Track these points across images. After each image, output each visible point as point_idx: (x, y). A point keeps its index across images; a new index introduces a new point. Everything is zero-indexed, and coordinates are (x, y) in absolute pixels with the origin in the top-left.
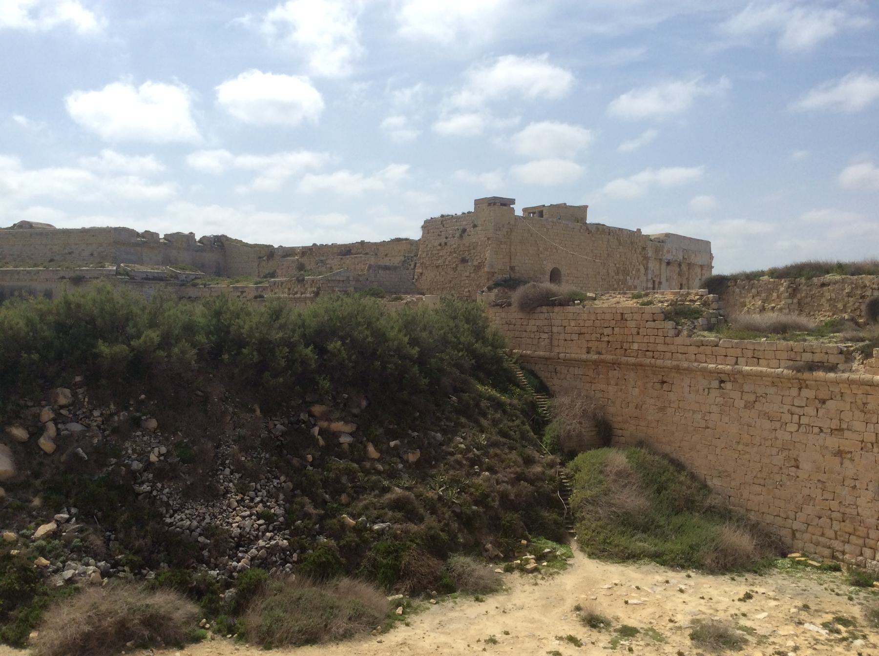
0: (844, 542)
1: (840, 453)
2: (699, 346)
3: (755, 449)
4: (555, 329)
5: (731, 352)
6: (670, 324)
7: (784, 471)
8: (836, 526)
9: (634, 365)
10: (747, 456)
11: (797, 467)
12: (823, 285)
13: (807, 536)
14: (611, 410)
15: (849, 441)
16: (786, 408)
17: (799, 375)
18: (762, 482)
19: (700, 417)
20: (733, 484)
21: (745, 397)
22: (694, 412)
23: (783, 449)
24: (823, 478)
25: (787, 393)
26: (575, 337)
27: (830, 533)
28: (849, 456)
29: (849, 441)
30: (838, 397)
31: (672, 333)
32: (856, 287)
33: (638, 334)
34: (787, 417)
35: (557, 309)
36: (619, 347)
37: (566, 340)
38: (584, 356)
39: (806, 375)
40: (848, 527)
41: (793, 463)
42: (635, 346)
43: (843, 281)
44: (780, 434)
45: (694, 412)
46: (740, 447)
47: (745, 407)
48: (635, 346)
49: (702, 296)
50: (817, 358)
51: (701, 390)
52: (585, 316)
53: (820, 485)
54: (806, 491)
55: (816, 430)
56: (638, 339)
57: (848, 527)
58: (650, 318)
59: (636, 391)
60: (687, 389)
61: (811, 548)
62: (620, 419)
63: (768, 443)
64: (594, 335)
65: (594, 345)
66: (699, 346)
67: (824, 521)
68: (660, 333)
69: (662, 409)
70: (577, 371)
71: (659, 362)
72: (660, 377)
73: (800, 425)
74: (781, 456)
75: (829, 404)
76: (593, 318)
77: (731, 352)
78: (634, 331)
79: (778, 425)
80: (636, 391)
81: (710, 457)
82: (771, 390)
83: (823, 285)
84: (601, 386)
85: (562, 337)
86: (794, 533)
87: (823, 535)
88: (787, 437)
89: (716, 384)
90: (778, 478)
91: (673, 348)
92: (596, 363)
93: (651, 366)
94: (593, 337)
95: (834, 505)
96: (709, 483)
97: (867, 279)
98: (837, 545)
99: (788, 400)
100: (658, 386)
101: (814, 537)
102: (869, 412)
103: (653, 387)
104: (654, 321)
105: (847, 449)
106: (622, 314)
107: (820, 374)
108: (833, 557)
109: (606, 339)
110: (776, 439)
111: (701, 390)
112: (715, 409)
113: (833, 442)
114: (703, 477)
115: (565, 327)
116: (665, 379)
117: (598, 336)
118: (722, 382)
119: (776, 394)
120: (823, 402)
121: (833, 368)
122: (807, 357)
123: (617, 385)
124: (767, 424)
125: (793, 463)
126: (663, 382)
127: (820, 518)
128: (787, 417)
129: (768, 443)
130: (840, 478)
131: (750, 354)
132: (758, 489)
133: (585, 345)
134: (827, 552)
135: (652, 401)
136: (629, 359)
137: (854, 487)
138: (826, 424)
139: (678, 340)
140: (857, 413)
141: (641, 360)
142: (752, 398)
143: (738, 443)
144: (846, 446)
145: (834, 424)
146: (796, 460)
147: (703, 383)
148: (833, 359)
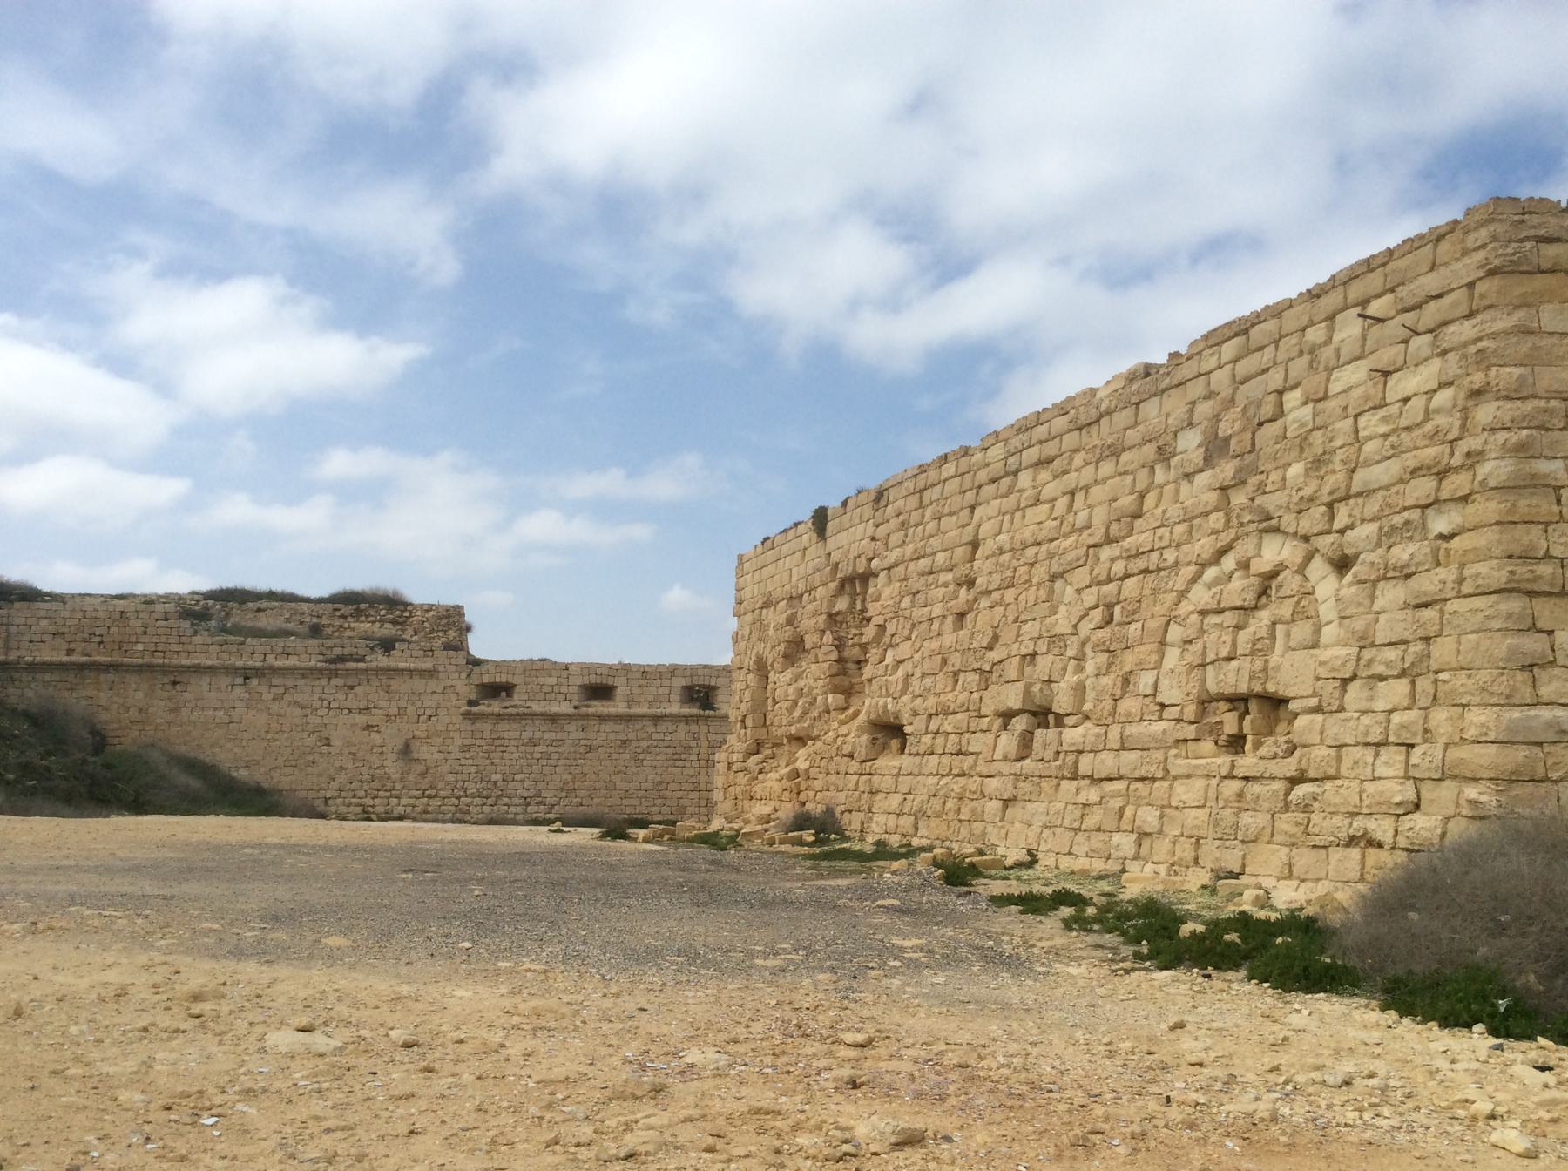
0: (373, 798)
1: (368, 727)
2: (221, 645)
3: (286, 735)
4: (13, 629)
5: (259, 649)
6: (186, 624)
7: (316, 750)
8: (366, 787)
9: (141, 666)
10: (278, 743)
11: (328, 745)
12: (259, 610)
13: (339, 801)
14: (104, 716)
15: (376, 717)
16: (317, 696)
17: (333, 666)
18: (294, 763)
19: (222, 713)
20: (262, 770)
21: (274, 690)
22: (215, 709)
23: (313, 732)
24: (354, 749)
25: (317, 683)
26: (47, 638)
27: (362, 793)
28: (376, 729)
29: (376, 717)
30: (365, 683)
31: (189, 632)
32: (296, 613)
33: (145, 633)
34: (317, 704)
35: (17, 605)
36: (117, 647)
37: (31, 642)
38: (65, 659)
39: (340, 666)
40: (376, 785)
41: (325, 741)
42: (140, 647)
43: (281, 608)
44: (311, 719)
45: (215, 709)
46: (270, 736)
47: (274, 699)
48: (140, 647)
49: (197, 601)
50: (347, 651)
51: (223, 687)
52: (67, 614)
53: (351, 756)
54: (337, 764)
55: (346, 711)
56: (146, 639)
57: (376, 785)
58: (161, 616)
59: (140, 695)
60: (206, 687)
61: (343, 809)
62: (115, 726)
63: (299, 728)
64: (80, 635)
65: (79, 647)
66: (221, 645)
67: (356, 785)
68: (174, 632)
69: (176, 710)
70: (47, 677)
71: (174, 661)
72: (172, 679)
73: (329, 709)
74: (314, 737)
75: (358, 689)
76: (80, 615)
77: (259, 649)
78: (140, 631)
79: (309, 711)
80: (140, 695)
81: (236, 750)
82: (301, 682)
83: (259, 610)
84: (90, 692)
85: (27, 638)
86: (326, 800)
87: (354, 796)
88: (319, 720)
89: (240, 680)
90: (310, 758)
91: (190, 648)
92: (81, 667)
93: (163, 665)
94: (79, 637)
95: (364, 770)
96: (234, 774)
97: (304, 607)
98: (368, 801)
99: (318, 690)
100: (169, 687)
101: (347, 800)
102: (392, 692)
103: (162, 689)
104: (166, 620)
105: (374, 724)
106: (122, 612)
107: (353, 665)
108: (364, 812)
109: (98, 639)
110: (308, 723)
111: (223, 687)
112: (239, 704)
113: (361, 719)
114: (226, 769)
115: (30, 627)
116: (178, 679)
117: (86, 636)
118: (246, 678)
119: (306, 685)
120: (351, 687)
121: (362, 659)
122: (338, 651)
123: (111, 689)
124: (298, 712)
125: (325, 741)
126: (175, 683)
127: (351, 783)
128: (317, 704)
129: (299, 728)
130: (369, 747)
131: (280, 650)
132: (288, 770)
133: (65, 646)
134: (359, 809)
135: (162, 703)
136: (135, 660)
137: (382, 753)
138: (354, 705)
139: (198, 639)
140: (382, 694)
141: (147, 660)
142: (281, 690)
143: (267, 732)
144: (373, 721)
145: (362, 705)
146: (328, 739)
147: (225, 681)
148: (361, 652)
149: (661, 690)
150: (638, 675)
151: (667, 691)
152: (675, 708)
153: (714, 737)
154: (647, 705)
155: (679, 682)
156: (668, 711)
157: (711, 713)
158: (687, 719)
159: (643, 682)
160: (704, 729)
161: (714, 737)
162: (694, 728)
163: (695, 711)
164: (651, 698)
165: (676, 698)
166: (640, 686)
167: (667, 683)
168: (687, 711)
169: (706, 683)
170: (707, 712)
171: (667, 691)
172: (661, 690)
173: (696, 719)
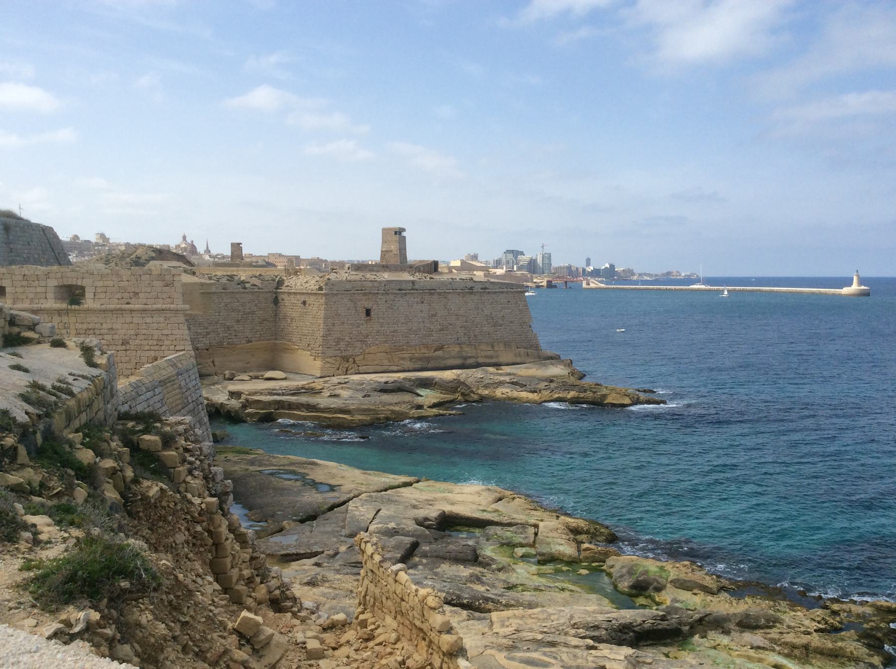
149: (39, 290)
150: (20, 278)
151: (43, 290)
152: (51, 303)
153: (80, 326)
154: (28, 301)
155: (52, 283)
156: (43, 306)
157: (77, 307)
158: (59, 312)
159: (25, 283)
160: (72, 320)
161: (80, 326)
162: (65, 319)
163: (64, 306)
164: (31, 296)
165: (51, 295)
166: (22, 286)
167: (43, 283)
168: (58, 306)
169: (74, 283)
170: (73, 307)
171: (43, 290)
172: (39, 289)
173: (67, 312)
